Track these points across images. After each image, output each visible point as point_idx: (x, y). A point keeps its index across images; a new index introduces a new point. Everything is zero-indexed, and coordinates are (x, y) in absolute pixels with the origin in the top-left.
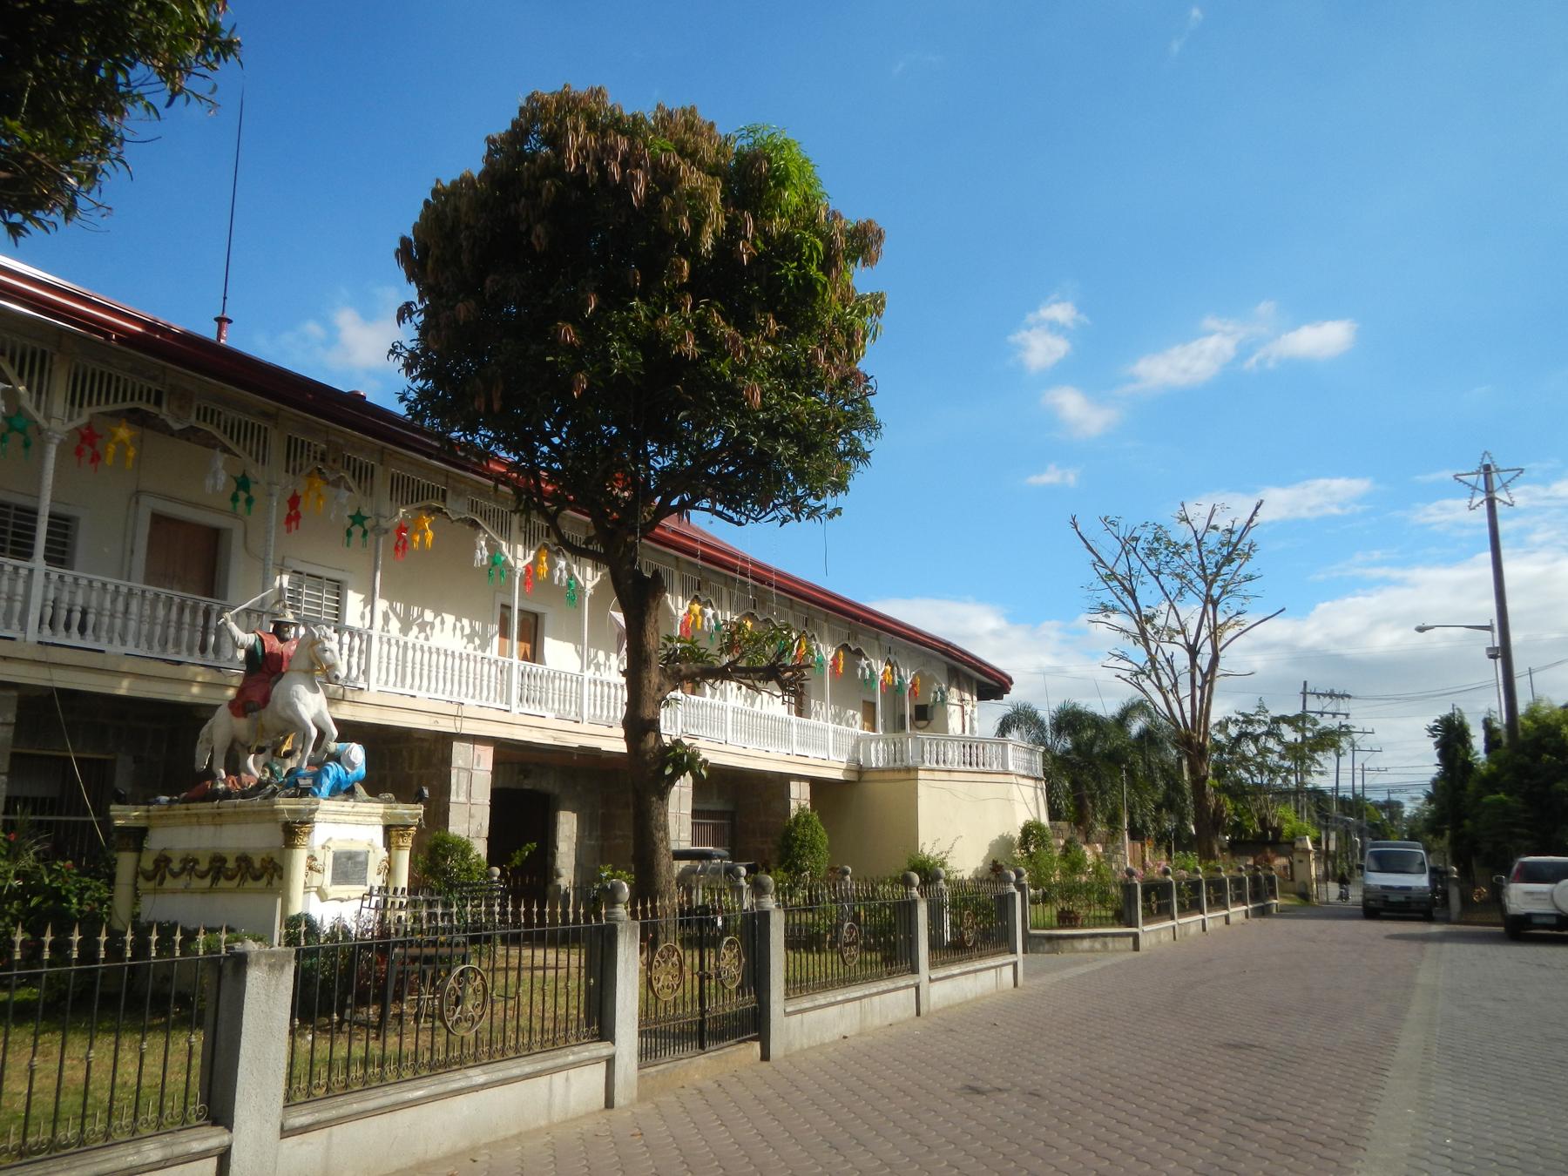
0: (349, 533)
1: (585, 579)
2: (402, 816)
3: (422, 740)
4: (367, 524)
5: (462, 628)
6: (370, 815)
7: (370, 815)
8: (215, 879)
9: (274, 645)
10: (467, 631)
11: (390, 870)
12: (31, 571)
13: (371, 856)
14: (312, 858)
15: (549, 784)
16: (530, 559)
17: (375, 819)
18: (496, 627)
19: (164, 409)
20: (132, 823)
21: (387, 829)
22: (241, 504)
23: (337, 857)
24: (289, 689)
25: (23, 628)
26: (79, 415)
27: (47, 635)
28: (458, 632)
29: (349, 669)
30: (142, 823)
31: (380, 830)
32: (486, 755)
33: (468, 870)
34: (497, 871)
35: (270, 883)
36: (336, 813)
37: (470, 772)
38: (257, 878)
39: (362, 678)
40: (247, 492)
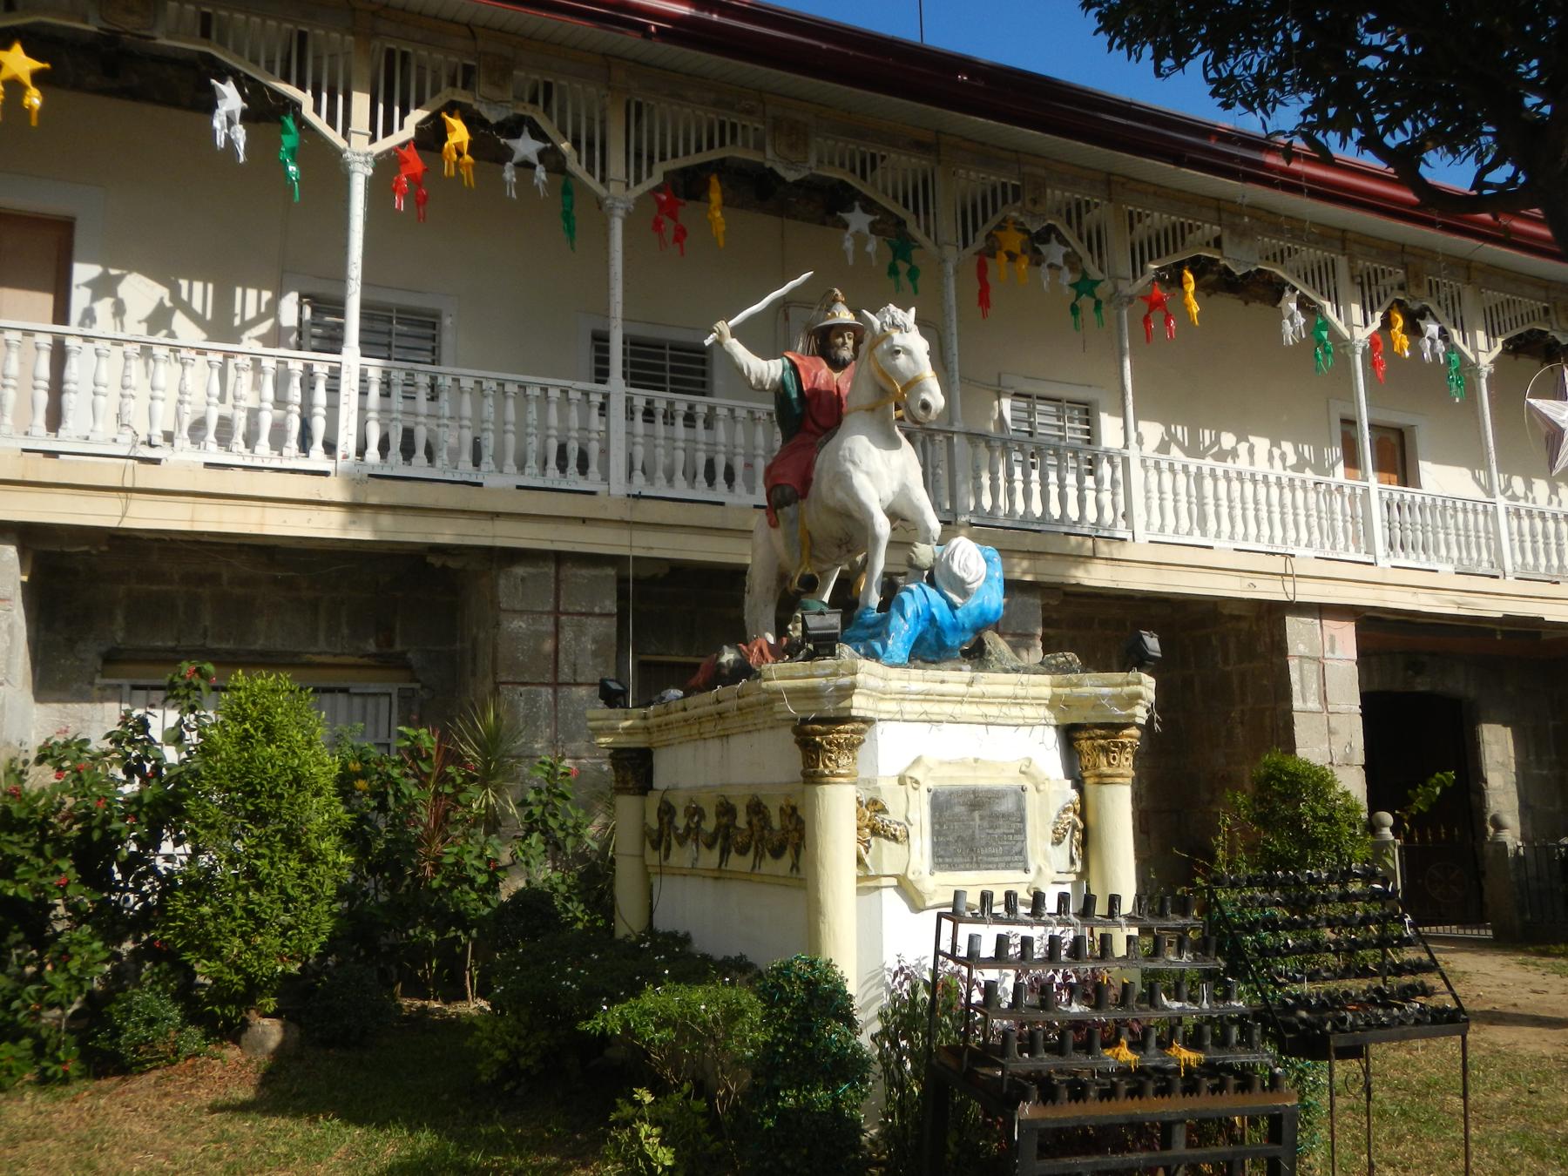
0: (1074, 309)
1: (1475, 350)
2: (1096, 702)
3: (1239, 618)
4: (1103, 291)
5: (1283, 457)
6: (1016, 700)
7: (1016, 700)
8: (724, 853)
9: (821, 375)
10: (1292, 459)
11: (1086, 837)
12: (606, 396)
13: (1032, 801)
14: (876, 806)
15: (1457, 683)
16: (1376, 324)
17: (1029, 712)
18: (1338, 451)
19: (769, 153)
20: (625, 742)
21: (1070, 735)
22: (903, 278)
23: (941, 804)
24: (838, 448)
25: (606, 478)
26: (650, 174)
27: (640, 484)
28: (1277, 462)
29: (1100, 509)
30: (639, 741)
31: (1051, 737)
32: (1345, 636)
33: (1330, 819)
34: (1387, 818)
35: (795, 866)
36: (926, 697)
37: (1320, 661)
38: (777, 853)
39: (1121, 524)
40: (908, 261)
